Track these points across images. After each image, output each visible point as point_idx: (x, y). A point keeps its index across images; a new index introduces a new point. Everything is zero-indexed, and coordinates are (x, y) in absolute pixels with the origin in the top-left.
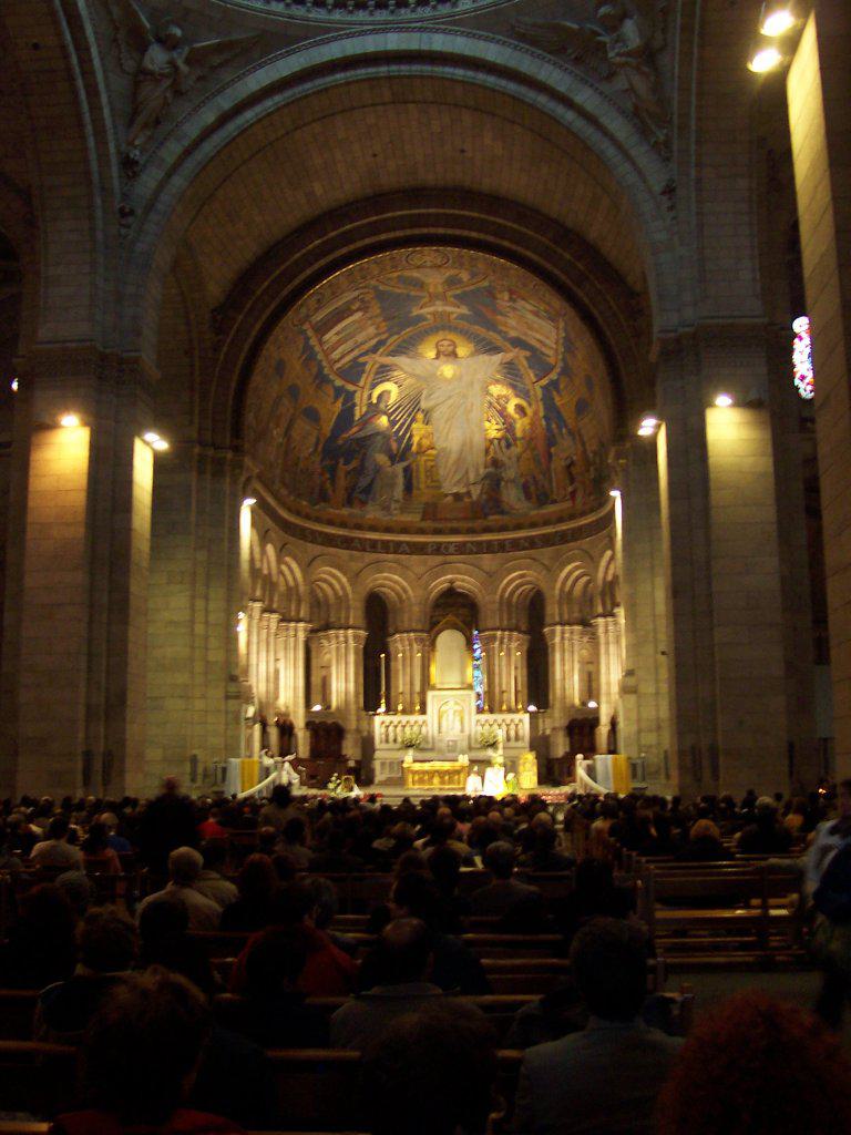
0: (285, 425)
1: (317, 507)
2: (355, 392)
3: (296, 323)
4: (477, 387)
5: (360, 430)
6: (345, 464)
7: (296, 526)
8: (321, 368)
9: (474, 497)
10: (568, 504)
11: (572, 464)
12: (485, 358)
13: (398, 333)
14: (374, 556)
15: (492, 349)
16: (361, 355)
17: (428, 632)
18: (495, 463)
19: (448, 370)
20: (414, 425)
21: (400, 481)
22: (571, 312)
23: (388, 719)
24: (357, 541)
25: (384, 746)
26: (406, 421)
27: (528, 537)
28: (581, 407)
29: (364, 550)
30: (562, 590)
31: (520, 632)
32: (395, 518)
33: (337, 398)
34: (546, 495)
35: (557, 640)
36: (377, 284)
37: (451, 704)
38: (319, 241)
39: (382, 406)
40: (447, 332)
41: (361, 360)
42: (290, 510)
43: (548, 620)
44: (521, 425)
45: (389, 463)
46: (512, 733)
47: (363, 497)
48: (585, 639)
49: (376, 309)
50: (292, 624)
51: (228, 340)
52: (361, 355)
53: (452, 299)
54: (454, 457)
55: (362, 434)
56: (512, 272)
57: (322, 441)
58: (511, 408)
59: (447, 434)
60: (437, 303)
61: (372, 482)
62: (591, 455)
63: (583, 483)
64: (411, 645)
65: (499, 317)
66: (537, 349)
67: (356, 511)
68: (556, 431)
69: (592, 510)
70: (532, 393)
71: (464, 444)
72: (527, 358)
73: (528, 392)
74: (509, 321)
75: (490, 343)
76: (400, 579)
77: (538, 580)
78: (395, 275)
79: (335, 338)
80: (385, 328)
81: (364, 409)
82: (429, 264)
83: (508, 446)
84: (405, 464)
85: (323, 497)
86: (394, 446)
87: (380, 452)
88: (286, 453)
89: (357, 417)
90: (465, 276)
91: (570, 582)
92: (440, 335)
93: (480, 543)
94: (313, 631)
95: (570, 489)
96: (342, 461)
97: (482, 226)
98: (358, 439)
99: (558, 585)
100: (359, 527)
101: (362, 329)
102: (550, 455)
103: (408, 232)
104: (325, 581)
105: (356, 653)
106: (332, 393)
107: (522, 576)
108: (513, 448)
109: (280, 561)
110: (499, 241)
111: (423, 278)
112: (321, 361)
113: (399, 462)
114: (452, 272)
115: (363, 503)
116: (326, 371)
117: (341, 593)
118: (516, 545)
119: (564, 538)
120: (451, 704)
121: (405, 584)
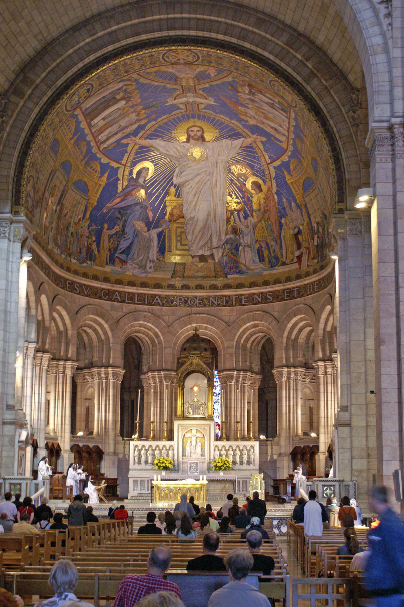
0: (59, 195)
1: (85, 264)
2: (118, 168)
3: (69, 108)
4: (221, 166)
5: (122, 201)
6: (107, 230)
7: (66, 280)
8: (89, 148)
9: (217, 261)
10: (296, 266)
11: (299, 232)
12: (229, 142)
13: (155, 120)
14: (132, 307)
15: (235, 135)
16: (124, 138)
17: (176, 371)
18: (235, 231)
19: (197, 152)
20: (167, 198)
21: (155, 243)
22: (302, 104)
23: (140, 443)
24: (117, 293)
25: (137, 466)
26: (160, 194)
27: (262, 293)
28: (308, 185)
29: (123, 301)
30: (288, 338)
31: (253, 372)
32: (149, 275)
33: (102, 174)
34: (277, 258)
35: (284, 379)
36: (138, 77)
37: (194, 432)
38: (90, 39)
39: (141, 181)
40: (196, 119)
41: (124, 141)
42: (61, 266)
43: (276, 363)
44: (257, 199)
46: (245, 458)
47: (123, 257)
48: (308, 380)
49: (136, 99)
50: (62, 363)
51: (11, 122)
52: (124, 138)
53: (201, 92)
54: (200, 225)
55: (123, 204)
56: (251, 69)
57: (90, 209)
58: (249, 185)
59: (195, 205)
60: (189, 95)
61: (131, 244)
62: (315, 225)
63: (308, 249)
64: (161, 382)
65: (240, 108)
66: (272, 135)
67: (117, 268)
68: (286, 205)
69: (315, 272)
71: (209, 215)
72: (262, 142)
73: (263, 171)
74: (248, 111)
75: (233, 129)
76: (153, 327)
77: (270, 329)
78: (155, 69)
79: (102, 123)
80: (145, 115)
81: (126, 183)
82: (182, 61)
83: (246, 217)
84: (160, 230)
85: (90, 256)
86: (151, 215)
87: (138, 220)
88: (59, 218)
89: (120, 189)
90: (212, 72)
91: (295, 332)
92: (190, 123)
93: (222, 297)
94: (78, 369)
95: (297, 253)
96: (106, 226)
97: (228, 30)
98: (119, 208)
99: (286, 334)
100: (119, 282)
101: (124, 115)
102: (281, 225)
103: (165, 34)
104: (90, 327)
105: (115, 387)
106: (99, 170)
107: (255, 326)
108: (250, 218)
109: (52, 309)
110: (241, 43)
111: (177, 74)
112: (89, 142)
113: (153, 228)
114: (201, 69)
115: (124, 262)
116: (94, 150)
117: (103, 337)
118: (251, 300)
119: (290, 294)
120: (194, 432)
121: (157, 331)
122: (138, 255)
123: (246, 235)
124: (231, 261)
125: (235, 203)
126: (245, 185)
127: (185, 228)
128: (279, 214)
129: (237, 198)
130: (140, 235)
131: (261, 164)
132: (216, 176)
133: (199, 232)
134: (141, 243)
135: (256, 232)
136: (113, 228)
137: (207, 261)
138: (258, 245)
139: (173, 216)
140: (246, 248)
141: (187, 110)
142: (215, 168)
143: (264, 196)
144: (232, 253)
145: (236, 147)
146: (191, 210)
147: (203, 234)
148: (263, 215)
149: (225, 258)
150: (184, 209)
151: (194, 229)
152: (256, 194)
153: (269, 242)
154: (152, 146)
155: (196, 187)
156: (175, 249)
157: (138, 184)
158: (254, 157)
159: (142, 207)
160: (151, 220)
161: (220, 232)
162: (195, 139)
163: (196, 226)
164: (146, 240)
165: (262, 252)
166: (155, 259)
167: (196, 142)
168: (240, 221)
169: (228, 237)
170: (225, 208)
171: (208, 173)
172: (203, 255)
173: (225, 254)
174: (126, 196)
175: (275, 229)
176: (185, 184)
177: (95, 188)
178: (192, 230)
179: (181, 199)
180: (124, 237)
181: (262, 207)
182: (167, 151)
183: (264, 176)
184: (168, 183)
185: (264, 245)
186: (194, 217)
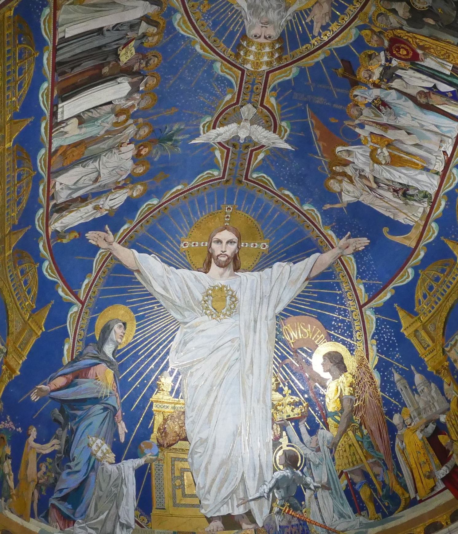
2: (71, 304)
6: (35, 441)
9: (260, 524)
34: (394, 499)
39: (108, 349)
45: (112, 457)
47: (66, 508)
54: (220, 453)
55: (70, 394)
59: (210, 413)
61: (83, 484)
68: (399, 386)
70: (357, 326)
72: (357, 254)
83: (312, 432)
84: (140, 462)
86: (122, 428)
87: (97, 436)
89: (66, 359)
96: (33, 432)
108: (322, 432)
113: (126, 459)
122: (96, 510)
123: (317, 466)
124: (290, 522)
125: (290, 404)
126: (309, 364)
127: (190, 460)
128: (384, 409)
129: (293, 393)
130: (100, 467)
131: (345, 310)
132: (253, 350)
133: (219, 468)
134: (104, 486)
135: (336, 457)
136: (47, 441)
137: (240, 527)
138: (346, 482)
139: (166, 434)
140: (320, 493)
141: (223, 177)
142: (252, 333)
143: (350, 379)
144: (290, 507)
145: (298, 279)
146: (201, 422)
147: (227, 474)
148: (350, 420)
149: (277, 518)
150: (187, 422)
151: (209, 463)
152: (334, 379)
153: (368, 469)
154: (138, 271)
155: (213, 375)
156: (171, 504)
157: (101, 356)
158: (333, 298)
159: (105, 409)
160: (122, 439)
161: (261, 467)
162: (220, 266)
163: (211, 456)
164: (112, 480)
165: (357, 493)
166: (132, 523)
167: (221, 270)
168: (301, 440)
169: (278, 474)
170: (270, 416)
171: (236, 344)
172: (229, 514)
173: (276, 509)
174: (77, 377)
175: (379, 442)
176: (190, 368)
177: (20, 333)
178: (204, 465)
179: (182, 401)
180: (69, 467)
181: (346, 404)
182: (165, 289)
183: (351, 337)
184: (158, 365)
185: (358, 479)
186: (207, 440)
